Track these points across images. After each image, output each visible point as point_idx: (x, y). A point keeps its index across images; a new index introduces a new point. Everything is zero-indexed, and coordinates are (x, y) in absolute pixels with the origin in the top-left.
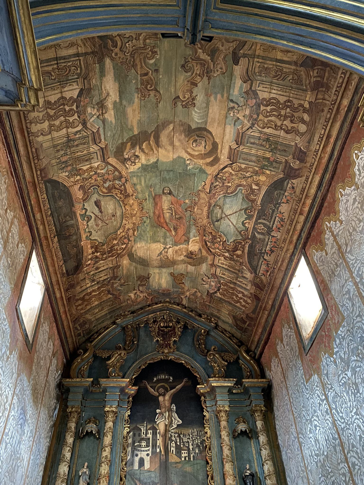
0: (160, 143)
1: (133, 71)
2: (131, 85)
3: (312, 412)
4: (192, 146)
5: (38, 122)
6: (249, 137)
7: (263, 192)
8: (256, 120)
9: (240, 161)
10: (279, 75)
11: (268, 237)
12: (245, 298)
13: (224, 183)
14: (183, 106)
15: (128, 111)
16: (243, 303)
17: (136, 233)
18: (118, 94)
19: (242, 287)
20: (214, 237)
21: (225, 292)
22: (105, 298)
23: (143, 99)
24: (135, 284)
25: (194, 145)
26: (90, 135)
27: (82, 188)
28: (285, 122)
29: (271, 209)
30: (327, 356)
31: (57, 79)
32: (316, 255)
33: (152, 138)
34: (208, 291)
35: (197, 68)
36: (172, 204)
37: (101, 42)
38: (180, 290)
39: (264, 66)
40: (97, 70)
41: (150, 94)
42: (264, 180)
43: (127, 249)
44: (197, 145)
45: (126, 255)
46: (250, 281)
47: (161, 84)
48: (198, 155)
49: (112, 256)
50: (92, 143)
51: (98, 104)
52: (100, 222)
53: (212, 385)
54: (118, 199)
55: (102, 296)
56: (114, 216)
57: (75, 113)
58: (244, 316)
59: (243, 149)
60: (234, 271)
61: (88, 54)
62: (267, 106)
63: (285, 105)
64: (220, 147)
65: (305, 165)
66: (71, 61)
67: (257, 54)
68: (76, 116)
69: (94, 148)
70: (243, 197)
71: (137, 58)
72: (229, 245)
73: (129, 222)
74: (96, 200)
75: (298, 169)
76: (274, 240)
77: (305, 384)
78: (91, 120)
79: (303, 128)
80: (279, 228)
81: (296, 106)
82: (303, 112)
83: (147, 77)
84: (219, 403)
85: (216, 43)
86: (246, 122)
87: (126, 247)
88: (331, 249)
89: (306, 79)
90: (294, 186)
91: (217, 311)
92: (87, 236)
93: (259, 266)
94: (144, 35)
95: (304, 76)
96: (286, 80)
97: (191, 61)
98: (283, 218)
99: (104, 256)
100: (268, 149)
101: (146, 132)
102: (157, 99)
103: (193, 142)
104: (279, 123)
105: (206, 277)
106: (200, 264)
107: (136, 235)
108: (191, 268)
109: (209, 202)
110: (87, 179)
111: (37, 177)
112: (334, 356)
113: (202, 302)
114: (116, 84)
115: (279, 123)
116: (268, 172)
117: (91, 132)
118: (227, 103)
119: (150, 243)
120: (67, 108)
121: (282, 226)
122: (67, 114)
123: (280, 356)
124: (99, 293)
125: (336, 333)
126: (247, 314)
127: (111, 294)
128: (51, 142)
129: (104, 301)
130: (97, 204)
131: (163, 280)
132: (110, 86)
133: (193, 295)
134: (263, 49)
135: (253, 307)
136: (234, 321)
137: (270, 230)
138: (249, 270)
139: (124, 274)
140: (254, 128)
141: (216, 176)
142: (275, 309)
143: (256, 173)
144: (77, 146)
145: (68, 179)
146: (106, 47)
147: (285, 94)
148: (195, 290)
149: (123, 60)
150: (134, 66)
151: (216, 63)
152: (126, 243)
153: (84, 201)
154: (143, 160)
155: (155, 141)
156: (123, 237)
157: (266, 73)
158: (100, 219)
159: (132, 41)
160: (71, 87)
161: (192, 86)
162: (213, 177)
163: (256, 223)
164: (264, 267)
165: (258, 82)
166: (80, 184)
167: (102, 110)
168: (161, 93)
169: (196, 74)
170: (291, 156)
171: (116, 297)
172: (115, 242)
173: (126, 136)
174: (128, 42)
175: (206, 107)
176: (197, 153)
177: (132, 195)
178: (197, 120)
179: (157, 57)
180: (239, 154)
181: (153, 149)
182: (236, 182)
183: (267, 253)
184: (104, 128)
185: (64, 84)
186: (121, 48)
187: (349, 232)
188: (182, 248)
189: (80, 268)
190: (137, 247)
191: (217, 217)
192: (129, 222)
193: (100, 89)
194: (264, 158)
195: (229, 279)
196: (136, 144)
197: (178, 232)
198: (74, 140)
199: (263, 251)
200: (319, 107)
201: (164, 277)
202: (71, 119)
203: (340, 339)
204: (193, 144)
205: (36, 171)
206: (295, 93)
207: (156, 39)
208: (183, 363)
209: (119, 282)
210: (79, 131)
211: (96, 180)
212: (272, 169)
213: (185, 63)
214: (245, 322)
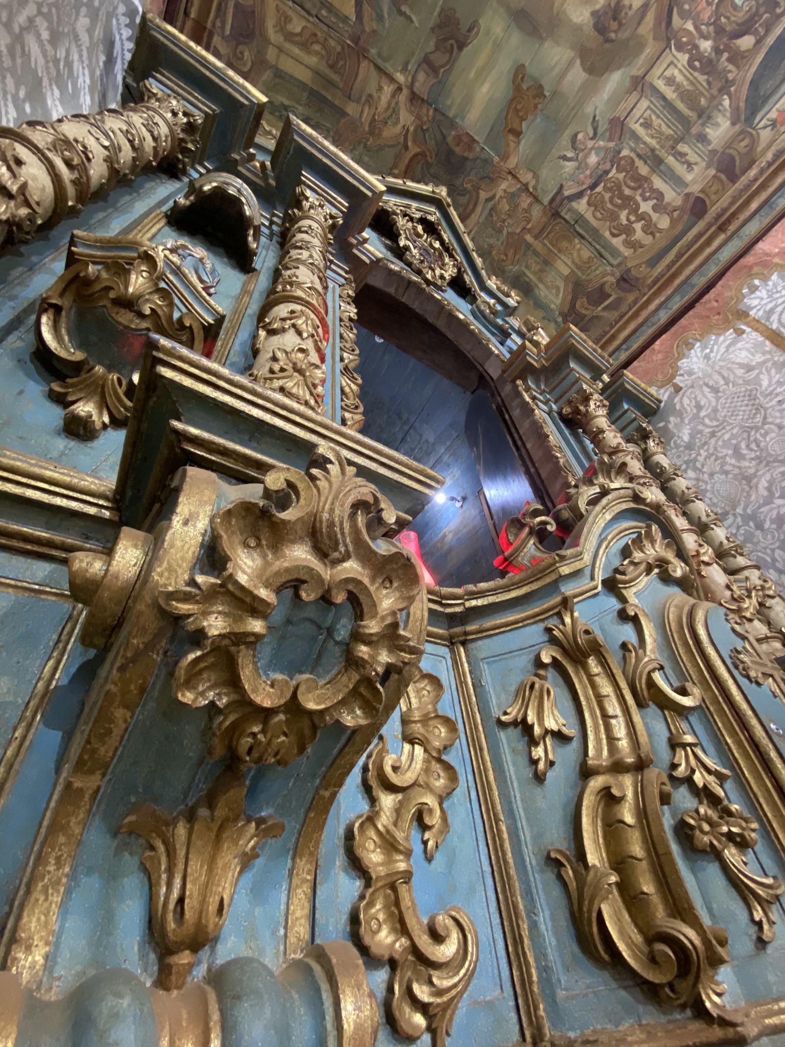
12: (655, 216)
16: (639, 234)
21: (607, 196)
34: (562, 187)
38: (496, 159)
91: (538, 267)
108: (577, 75)
113: (518, 231)
126: (629, 270)
131: (485, 89)
133: (512, 197)
135: (664, 243)
136: (570, 297)
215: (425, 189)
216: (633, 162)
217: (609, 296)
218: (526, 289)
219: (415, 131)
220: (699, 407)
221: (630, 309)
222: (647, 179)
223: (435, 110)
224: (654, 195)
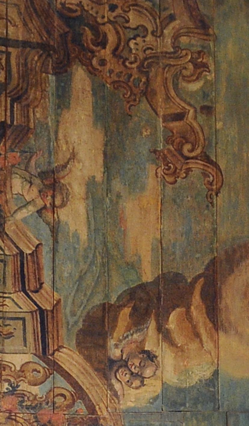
1: (144, 105)
15: (128, 212)
18: (100, 160)
23: (171, 179)
26: (10, 259)
33: (196, 299)
37: (67, 30)
41: (188, 170)
47: (219, 145)
50: (14, 285)
51: (43, 175)
71: (156, 76)
83: (182, 123)
101: (177, 275)
102: (211, 184)
114: (98, 132)
117: (15, 251)
132: (80, 136)
146: (77, 40)
149: (119, 77)
150: (148, 93)
155: (207, 308)
159: (144, 37)
167: (53, 197)
173: (118, 288)
174: (134, 38)
179: (208, 78)
184: (54, 251)
186: (116, 49)
207: (205, 37)
211: (9, 418)
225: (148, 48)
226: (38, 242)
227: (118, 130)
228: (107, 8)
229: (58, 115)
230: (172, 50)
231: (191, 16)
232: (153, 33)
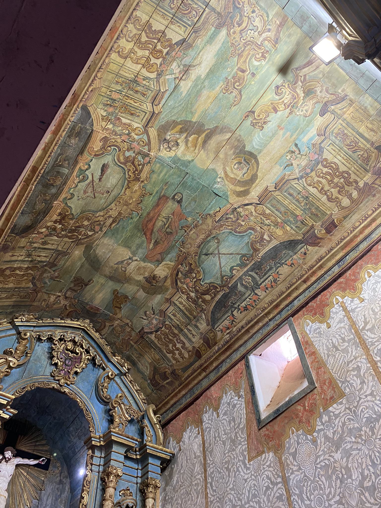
0: (207, 145)
1: (236, 59)
2: (224, 71)
3: (248, 498)
4: (233, 166)
5: (125, 37)
6: (291, 187)
7: (271, 246)
8: (307, 174)
9: (268, 205)
10: (352, 145)
11: (250, 292)
12: (183, 351)
13: (238, 219)
14: (251, 123)
16: (177, 356)
17: (114, 225)
19: (188, 336)
20: (191, 271)
22: (23, 285)
23: (224, 92)
24: (65, 286)
25: (235, 167)
27: (105, 139)
28: (332, 190)
29: (269, 265)
30: (300, 432)
31: (173, 10)
32: (309, 326)
33: (204, 134)
34: (143, 328)
35: (287, 97)
36: (173, 214)
37: (232, 11)
39: (344, 131)
40: (209, 34)
41: (232, 92)
42: (280, 234)
43: (91, 238)
44: (238, 168)
45: (84, 245)
46: (201, 333)
47: (247, 90)
48: (232, 178)
49: (70, 238)
51: (185, 66)
52: (90, 190)
53: (113, 438)
54: (127, 176)
55: (22, 280)
56: (109, 192)
57: (160, 58)
58: (169, 371)
59: (278, 195)
60: (189, 315)
61: (214, 12)
62: (325, 167)
63: (341, 175)
64: (257, 182)
65: (330, 237)
66: (198, 4)
67: (345, 116)
68: (159, 62)
69: (147, 107)
70: (248, 242)
71: (247, 50)
72: (201, 285)
73: (116, 209)
74: (106, 162)
75: (321, 239)
76: (255, 297)
77: (247, 462)
78: (167, 77)
79: (346, 202)
80: (267, 288)
81: (351, 180)
82: (354, 189)
83: (242, 74)
84: (112, 463)
85: (317, 86)
86: (297, 171)
87: (91, 236)
88: (338, 323)
89: (373, 162)
90: (307, 252)
91: (137, 356)
92: (66, 197)
93: (222, 321)
94: (267, 35)
95: (373, 159)
96: (356, 154)
97: (286, 86)
98: (278, 279)
99: (62, 233)
100: (301, 206)
101: (203, 125)
102: (235, 101)
103: (236, 163)
104: (326, 188)
105: (151, 311)
106: (155, 293)
107: (112, 228)
108: (141, 294)
109: (210, 231)
110: (116, 134)
111: (86, 92)
112: (315, 434)
115: (326, 188)
116: (288, 228)
118: (291, 144)
119: (119, 245)
120: (159, 47)
121: (272, 286)
122: (155, 52)
123: (205, 425)
124: (23, 274)
125: (325, 409)
126: (175, 370)
127: (32, 283)
128: (119, 68)
129: (20, 288)
130: (104, 168)
131: (101, 295)
133: (121, 327)
134: (353, 116)
135: (187, 364)
136: (152, 373)
137: (257, 285)
138: (207, 320)
139: (65, 266)
140: (300, 181)
141: (236, 209)
142: (218, 372)
143: (276, 224)
144: (137, 92)
145: (101, 120)
147: (348, 165)
148: (128, 321)
149: (236, 42)
151: (306, 103)
152: (96, 231)
153: (95, 155)
154: (180, 151)
155: (204, 140)
156: (98, 223)
157: (342, 139)
158: (93, 187)
160: (177, 29)
161: (272, 110)
162: (232, 207)
163: (245, 274)
164: (227, 323)
165: (330, 142)
166: (106, 135)
167: (183, 75)
168: (243, 98)
169: (283, 101)
170: (319, 223)
171: (36, 291)
172: (86, 223)
175: (271, 138)
176: (232, 176)
177: (142, 182)
178: (254, 144)
179: (263, 63)
180: (271, 198)
181: (196, 147)
182: (252, 223)
183: (239, 309)
185: (176, 21)
186: (242, 30)
187: (373, 311)
188: (149, 267)
189: (30, 231)
190: (103, 242)
191: (208, 251)
192: (116, 209)
193: (197, 53)
194: (292, 213)
195: (178, 323)
196: (186, 131)
197: (156, 248)
198: (138, 84)
199: (235, 306)
200: (372, 190)
201: (104, 292)
202: (153, 60)
203: (330, 417)
204: (235, 165)
205: (90, 85)
206: (357, 168)
207: (273, 46)
208: (78, 402)
209: (53, 273)
210: (150, 79)
212: (294, 228)
213: (281, 86)
214: (166, 378)
215: (75, 323)
216: (171, 327)
217: (168, 378)
218: (133, 363)
219: (70, 305)
220: (182, 467)
221: (172, 393)
222: (178, 335)
223: (78, 300)
224: (181, 342)
225: (253, 37)
226: (167, 89)
227: (221, 63)
228: (251, 10)
229: (205, 45)
230: (260, 44)
231: (276, 35)
232: (259, 32)
